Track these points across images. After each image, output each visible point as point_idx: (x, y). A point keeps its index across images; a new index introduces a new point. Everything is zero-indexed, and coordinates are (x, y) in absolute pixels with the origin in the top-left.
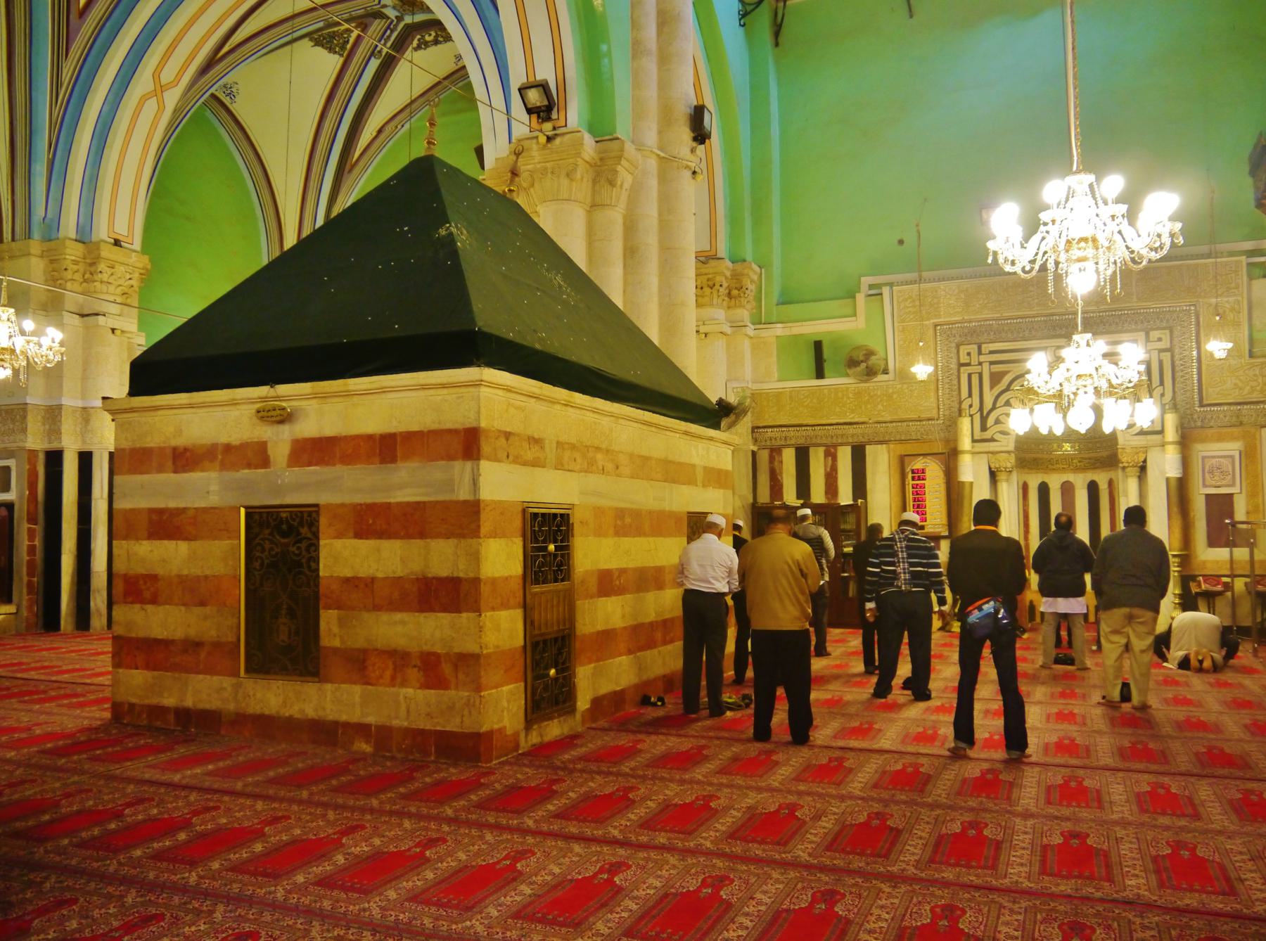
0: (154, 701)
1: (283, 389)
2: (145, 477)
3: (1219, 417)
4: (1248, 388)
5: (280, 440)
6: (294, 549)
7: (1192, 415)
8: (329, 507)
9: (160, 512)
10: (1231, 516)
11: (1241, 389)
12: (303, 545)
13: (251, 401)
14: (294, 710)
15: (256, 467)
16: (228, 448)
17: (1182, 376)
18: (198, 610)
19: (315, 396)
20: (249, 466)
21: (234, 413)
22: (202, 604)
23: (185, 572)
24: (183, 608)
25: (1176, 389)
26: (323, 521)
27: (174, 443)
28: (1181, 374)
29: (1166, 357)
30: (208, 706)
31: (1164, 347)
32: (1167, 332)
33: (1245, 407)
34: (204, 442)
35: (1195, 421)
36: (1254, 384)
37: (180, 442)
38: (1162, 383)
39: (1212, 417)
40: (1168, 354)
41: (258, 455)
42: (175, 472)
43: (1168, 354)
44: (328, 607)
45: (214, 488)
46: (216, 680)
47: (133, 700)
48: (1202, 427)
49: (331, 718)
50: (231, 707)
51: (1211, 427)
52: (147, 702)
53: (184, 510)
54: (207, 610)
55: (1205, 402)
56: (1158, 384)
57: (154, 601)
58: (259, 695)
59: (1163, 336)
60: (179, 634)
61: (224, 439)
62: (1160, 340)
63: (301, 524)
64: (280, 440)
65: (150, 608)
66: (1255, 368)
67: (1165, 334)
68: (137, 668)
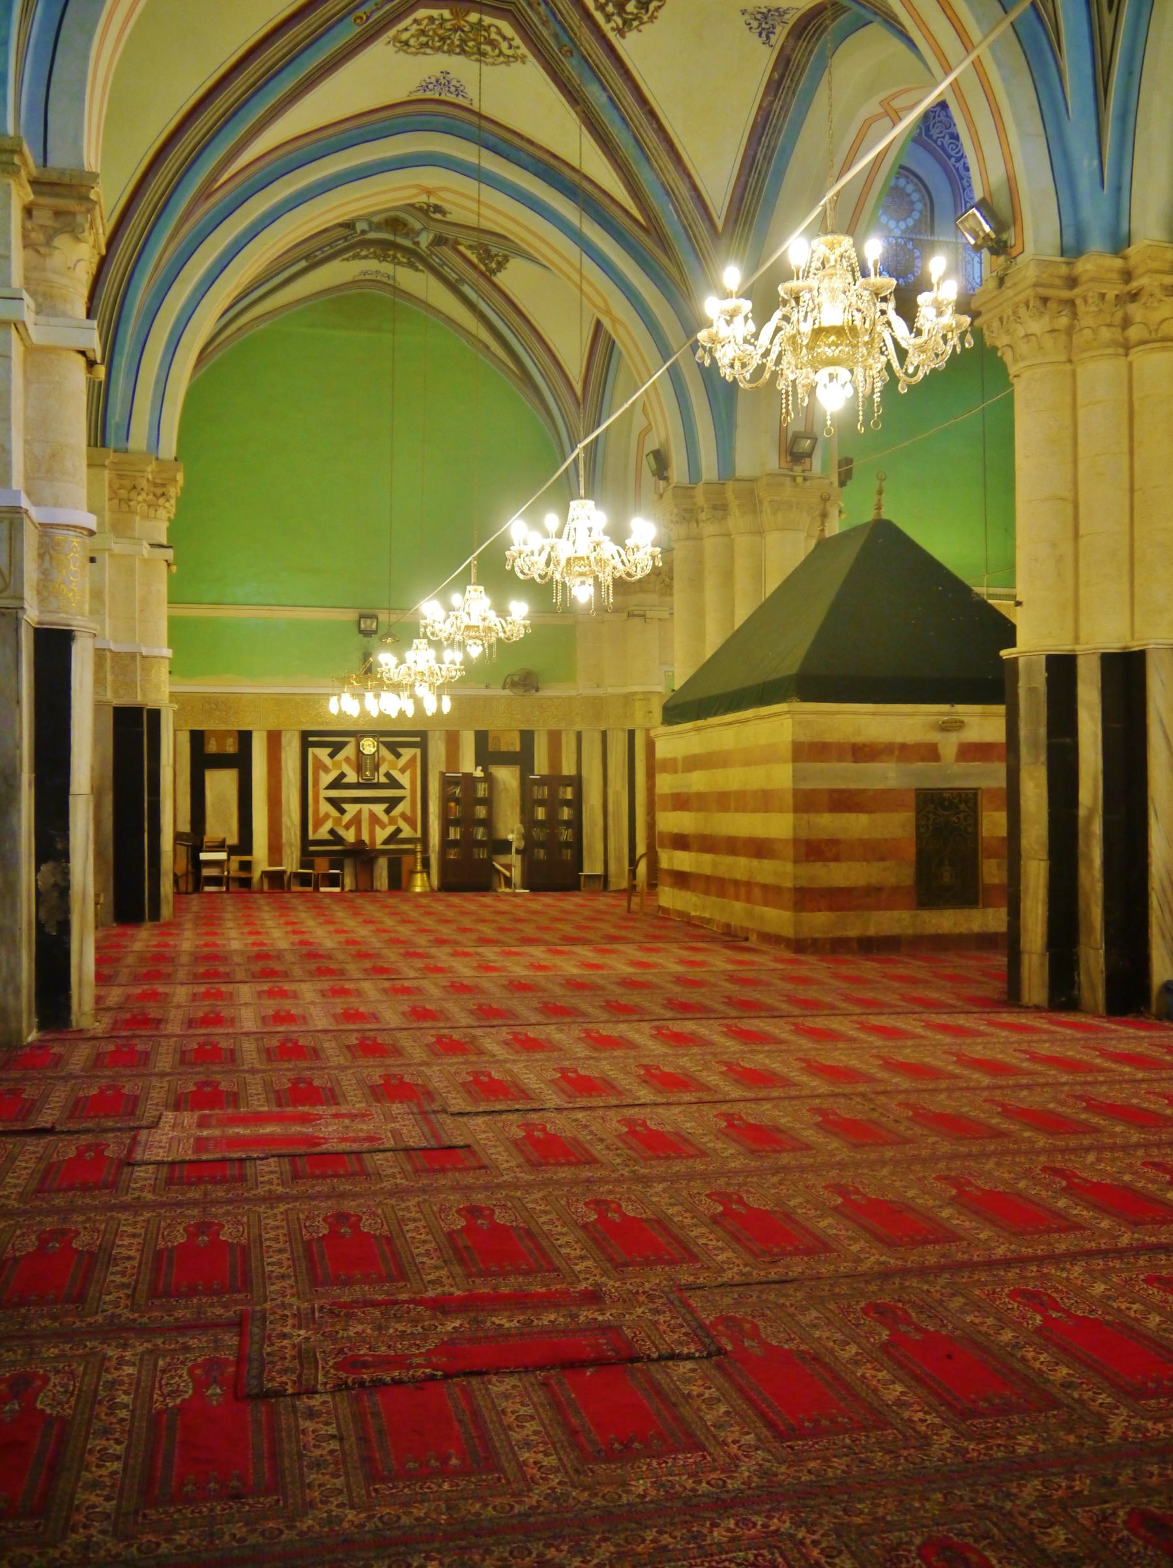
0: (838, 933)
1: (960, 708)
2: (824, 765)
5: (949, 745)
6: (954, 818)
8: (989, 790)
9: (841, 792)
12: (961, 816)
13: (928, 714)
14: (963, 929)
15: (930, 761)
16: (903, 747)
18: (882, 864)
19: (984, 715)
20: (923, 760)
21: (909, 721)
22: (882, 859)
23: (866, 837)
24: (865, 864)
26: (983, 801)
27: (853, 740)
30: (888, 933)
34: (881, 740)
37: (860, 739)
41: (931, 753)
42: (855, 762)
44: (989, 857)
45: (892, 774)
46: (895, 914)
47: (817, 935)
49: (992, 930)
50: (910, 931)
52: (831, 935)
53: (864, 791)
54: (888, 864)
57: (836, 859)
58: (933, 921)
60: (862, 882)
61: (899, 739)
63: (960, 801)
64: (949, 745)
65: (832, 865)
68: (820, 911)
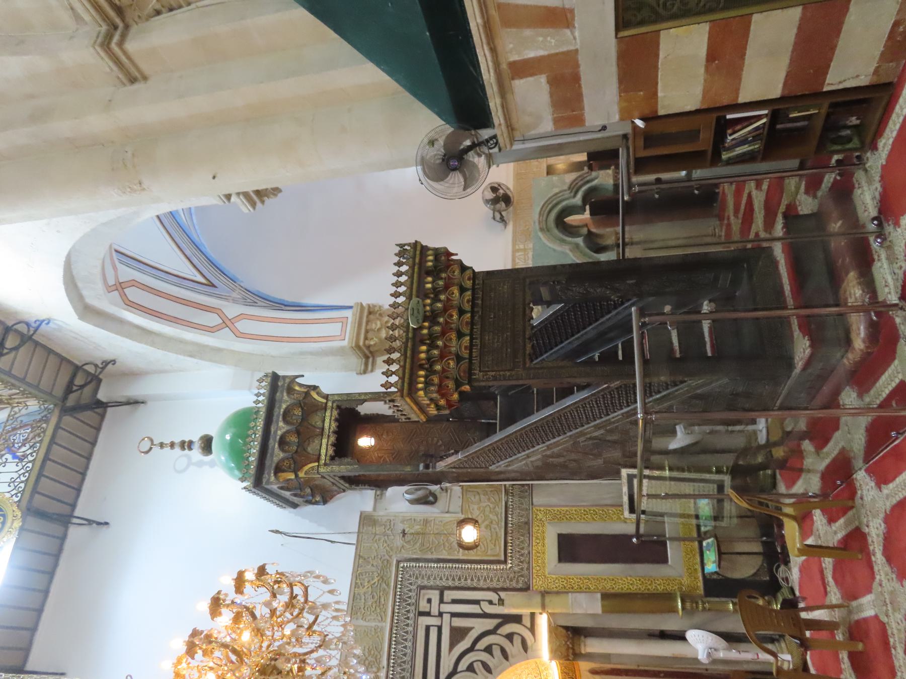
3: (519, 545)
4: (491, 516)
7: (515, 572)
10: (629, 537)
11: (492, 522)
17: (472, 580)
25: (485, 587)
28: (469, 581)
29: (449, 595)
31: (438, 597)
32: (423, 592)
33: (510, 519)
35: (522, 569)
36: (488, 509)
38: (477, 602)
39: (519, 552)
40: (446, 593)
43: (446, 593)
48: (529, 563)
51: (529, 553)
55: (502, 558)
56: (477, 606)
59: (427, 597)
62: (429, 601)
66: (471, 508)
67: (424, 595)
